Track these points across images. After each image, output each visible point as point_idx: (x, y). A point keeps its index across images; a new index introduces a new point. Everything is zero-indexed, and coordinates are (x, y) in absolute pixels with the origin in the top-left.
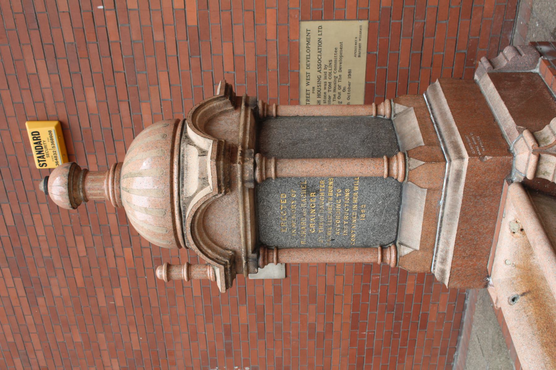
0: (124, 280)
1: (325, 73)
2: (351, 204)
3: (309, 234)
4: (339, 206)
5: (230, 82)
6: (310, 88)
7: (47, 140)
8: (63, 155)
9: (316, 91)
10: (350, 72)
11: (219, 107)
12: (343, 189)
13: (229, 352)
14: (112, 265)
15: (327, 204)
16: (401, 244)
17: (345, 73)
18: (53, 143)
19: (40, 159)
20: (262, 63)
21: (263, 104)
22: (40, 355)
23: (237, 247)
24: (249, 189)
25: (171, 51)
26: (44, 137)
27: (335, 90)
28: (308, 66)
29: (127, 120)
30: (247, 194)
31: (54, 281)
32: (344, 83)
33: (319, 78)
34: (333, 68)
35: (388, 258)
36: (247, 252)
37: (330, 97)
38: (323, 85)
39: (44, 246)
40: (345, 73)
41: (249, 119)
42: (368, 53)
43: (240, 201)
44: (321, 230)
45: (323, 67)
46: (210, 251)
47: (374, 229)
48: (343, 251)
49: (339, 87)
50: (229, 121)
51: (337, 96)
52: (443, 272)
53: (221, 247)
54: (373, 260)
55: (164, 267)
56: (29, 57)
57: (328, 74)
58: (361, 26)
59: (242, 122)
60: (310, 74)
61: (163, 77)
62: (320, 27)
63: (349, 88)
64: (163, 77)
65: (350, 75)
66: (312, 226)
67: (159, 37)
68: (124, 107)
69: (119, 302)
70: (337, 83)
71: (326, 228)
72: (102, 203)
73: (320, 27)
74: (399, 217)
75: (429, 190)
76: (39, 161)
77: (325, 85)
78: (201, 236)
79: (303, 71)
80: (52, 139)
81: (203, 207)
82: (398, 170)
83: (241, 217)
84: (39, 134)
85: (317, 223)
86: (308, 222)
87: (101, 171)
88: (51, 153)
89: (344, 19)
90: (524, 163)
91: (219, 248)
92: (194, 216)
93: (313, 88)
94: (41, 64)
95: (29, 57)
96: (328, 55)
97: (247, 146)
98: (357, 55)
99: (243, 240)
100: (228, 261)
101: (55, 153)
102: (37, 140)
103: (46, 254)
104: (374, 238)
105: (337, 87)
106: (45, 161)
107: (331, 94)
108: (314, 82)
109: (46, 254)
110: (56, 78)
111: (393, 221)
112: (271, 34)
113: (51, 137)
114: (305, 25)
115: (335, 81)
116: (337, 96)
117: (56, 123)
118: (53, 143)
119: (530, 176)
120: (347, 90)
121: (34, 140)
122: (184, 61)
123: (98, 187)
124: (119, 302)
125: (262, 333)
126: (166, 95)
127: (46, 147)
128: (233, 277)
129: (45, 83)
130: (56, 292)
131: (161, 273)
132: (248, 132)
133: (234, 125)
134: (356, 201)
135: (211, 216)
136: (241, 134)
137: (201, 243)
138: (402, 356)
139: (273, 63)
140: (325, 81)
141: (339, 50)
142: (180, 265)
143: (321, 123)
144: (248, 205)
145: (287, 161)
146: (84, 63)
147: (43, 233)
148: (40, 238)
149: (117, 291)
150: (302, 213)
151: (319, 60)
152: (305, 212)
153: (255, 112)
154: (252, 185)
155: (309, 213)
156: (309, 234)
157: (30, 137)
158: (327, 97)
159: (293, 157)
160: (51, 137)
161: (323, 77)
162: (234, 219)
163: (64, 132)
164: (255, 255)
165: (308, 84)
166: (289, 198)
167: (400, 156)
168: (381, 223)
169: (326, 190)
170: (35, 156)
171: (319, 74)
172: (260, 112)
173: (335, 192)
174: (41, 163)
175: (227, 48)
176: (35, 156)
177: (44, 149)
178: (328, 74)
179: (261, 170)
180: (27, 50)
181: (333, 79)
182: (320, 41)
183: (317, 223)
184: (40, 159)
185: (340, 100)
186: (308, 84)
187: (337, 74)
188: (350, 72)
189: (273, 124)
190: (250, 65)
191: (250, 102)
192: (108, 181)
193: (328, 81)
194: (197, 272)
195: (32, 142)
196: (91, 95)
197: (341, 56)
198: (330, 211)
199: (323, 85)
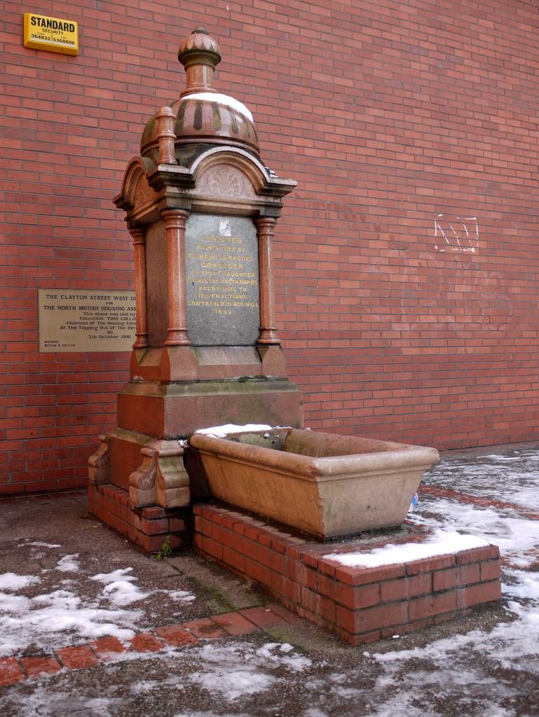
1: (127, 314)
2: (232, 301)
6: (112, 300)
7: (63, 36)
9: (108, 305)
12: (246, 293)
15: (231, 279)
19: (41, 21)
24: (258, 211)
26: (68, 35)
27: (109, 323)
29: (77, 121)
32: (116, 332)
33: (121, 309)
37: (102, 319)
38: (116, 312)
47: (206, 323)
49: (113, 328)
51: (103, 326)
56: (142, 52)
70: (116, 326)
76: (39, 19)
78: (218, 160)
80: (64, 41)
84: (71, 31)
88: (47, 34)
93: (112, 303)
95: (142, 52)
102: (65, 27)
104: (196, 324)
105: (113, 326)
106: (39, 25)
107: (106, 320)
108: (117, 303)
110: (122, 68)
111: (215, 340)
113: (67, 42)
116: (103, 326)
120: (110, 335)
121: (65, 24)
126: (104, 164)
127: (55, 32)
129: (117, 57)
134: (235, 304)
140: (119, 314)
144: (244, 207)
157: (69, 22)
160: (67, 42)
163: (69, 55)
165: (116, 298)
168: (212, 329)
169: (246, 279)
170: (46, 18)
174: (37, 20)
176: (46, 18)
177: (52, 29)
180: (150, 54)
181: (122, 322)
184: (41, 21)
185: (98, 328)
186: (116, 298)
187: (125, 325)
193: (119, 317)
195: (63, 21)
199: (116, 312)
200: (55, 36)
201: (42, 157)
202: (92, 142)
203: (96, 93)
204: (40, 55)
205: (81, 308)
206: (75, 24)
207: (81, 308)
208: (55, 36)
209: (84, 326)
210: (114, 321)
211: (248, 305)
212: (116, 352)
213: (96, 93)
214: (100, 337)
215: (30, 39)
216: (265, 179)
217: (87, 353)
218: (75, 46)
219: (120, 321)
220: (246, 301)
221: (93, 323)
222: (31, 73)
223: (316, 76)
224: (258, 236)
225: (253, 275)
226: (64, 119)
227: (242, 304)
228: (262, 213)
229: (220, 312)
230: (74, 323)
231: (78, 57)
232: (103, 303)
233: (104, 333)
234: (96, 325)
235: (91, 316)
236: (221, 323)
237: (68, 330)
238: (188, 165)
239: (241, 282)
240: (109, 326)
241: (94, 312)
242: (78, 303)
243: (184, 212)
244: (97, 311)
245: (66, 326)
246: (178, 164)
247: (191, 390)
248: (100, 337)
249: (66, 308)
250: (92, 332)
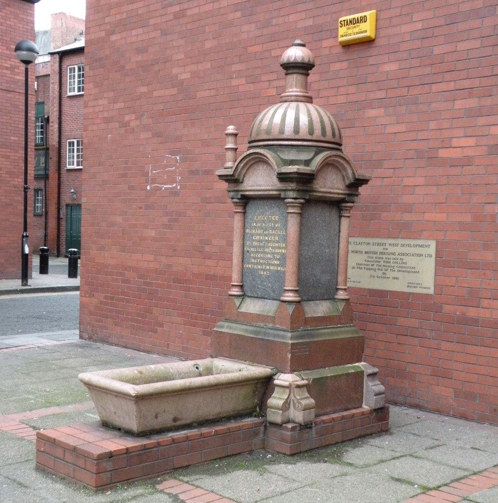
0: (251, 87)
2: (270, 265)
3: (252, 235)
5: (369, 183)
6: (387, 246)
8: (349, 41)
9: (384, 251)
10: (397, 278)
11: (347, 174)
13: (192, 172)
14: (265, 78)
16: (243, 299)
17: (396, 274)
18: (357, 33)
20: (408, 208)
21: (351, 207)
22: (196, 11)
23: (245, 184)
24: (280, 194)
25: (421, 135)
27: (384, 266)
28: (403, 245)
29: (372, 96)
31: (253, 26)
32: (390, 274)
33: (394, 254)
34: (401, 265)
35: (234, 290)
36: (241, 191)
37: (380, 262)
38: (389, 256)
39: (281, 20)
40: (396, 274)
41: (336, 196)
42: (410, 294)
43: (273, 188)
44: (255, 244)
45: (402, 257)
46: (242, 165)
48: (240, 260)
50: (335, 182)
52: (222, 327)
53: (246, 172)
54: (233, 279)
55: (235, 132)
57: (397, 261)
58: (430, 288)
59: (332, 191)
60: (397, 247)
61: (402, 128)
62: (431, 256)
63: (385, 278)
64: (402, 128)
65: (394, 278)
66: (258, 237)
67: (433, 125)
68: (381, 94)
69: (235, 82)
70: (389, 268)
71: (255, 247)
72: (283, 89)
73: (431, 256)
74: (260, 298)
75: (274, 317)
76: (344, 21)
77: (389, 259)
79: (400, 241)
81: (270, 162)
82: (288, 296)
83: (263, 188)
86: (260, 235)
87: (306, 86)
88: (350, 31)
89: (436, 275)
90: (284, 379)
91: (245, 171)
92: (264, 155)
93: (387, 249)
94: (419, 26)
96: (411, 261)
97: (312, 194)
98: (410, 285)
99: (249, 188)
100: (236, 177)
101: (350, 35)
102: (361, 20)
103: (274, 21)
107: (382, 263)
108: (391, 249)
109: (274, 21)
112: (427, 216)
114: (433, 244)
115: (391, 266)
116: (380, 267)
117: (373, 36)
118: (357, 33)
119: (276, 382)
120: (384, 276)
121: (360, 17)
122: (414, 145)
123: (294, 85)
124: (235, 82)
125: (206, 201)
127: (355, 27)
128: (227, 181)
129: (405, 28)
130: (245, 28)
131: (231, 129)
132: (324, 195)
133: (331, 185)
135: (265, 166)
136: (322, 190)
137: (247, 159)
138: (183, 315)
139: (407, 217)
141: (414, 270)
142: (236, 143)
143: (334, 247)
144: (271, 193)
145: (298, 221)
146: (416, 62)
147: (290, 20)
148: (287, 17)
149: (243, 81)
150: (265, 230)
151: (413, 255)
152: (266, 232)
153: (343, 201)
154: (282, 196)
155: (266, 235)
156: (252, 235)
157: (362, 14)
158: (380, 260)
159: (301, 225)
160: (362, 32)
161: (394, 257)
162: (263, 183)
163: (368, 42)
164: (239, 197)
165: (390, 245)
166: (276, 222)
167: (297, 299)
169: (279, 248)
171: (397, 254)
172: (344, 205)
173: (278, 253)
174: (343, 23)
175: (420, 181)
177: (353, 26)
178: (397, 261)
179: (292, 203)
182: (421, 255)
186: (390, 245)
187: (396, 269)
188: (397, 278)
189: (334, 213)
190: (407, 199)
191: (351, 198)
192: (297, 92)
193: (392, 261)
194: (230, 155)
197: (409, 272)
198: (266, 250)
199: (389, 256)
200: (356, 30)
205: (366, 253)
207: (366, 253)
208: (356, 30)
209: (367, 267)
210: (388, 264)
211: (279, 268)
212: (388, 291)
214: (378, 277)
215: (340, 39)
217: (368, 289)
219: (392, 265)
220: (278, 265)
221: (373, 265)
222: (344, 65)
229: (262, 273)
230: (360, 265)
231: (376, 40)
232: (380, 249)
233: (380, 273)
234: (375, 267)
235: (372, 260)
236: (263, 281)
237: (357, 270)
240: (384, 268)
241: (374, 256)
242: (364, 248)
244: (376, 256)
245: (356, 266)
248: (378, 277)
249: (357, 252)
250: (372, 273)
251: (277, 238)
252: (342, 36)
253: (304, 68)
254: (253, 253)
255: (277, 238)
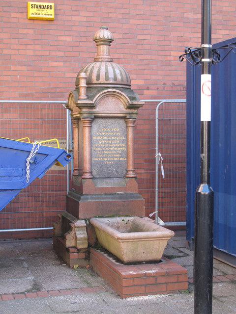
4: (113, 152)
12: (120, 154)
18: (45, 15)
29: (54, 54)
30: (124, 115)
52: (87, 199)
68: (61, 54)
76: (35, 5)
85: (104, 144)
101: (39, 14)
118: (45, 15)
129: (74, 18)
157: (49, 4)
160: (49, 15)
164: (93, 117)
173: (119, 150)
174: (34, 6)
183: (104, 144)
196: (68, 39)
200: (43, 12)
201: (36, 74)
202: (62, 64)
203: (64, 38)
204: (36, 22)
206: (52, 4)
208: (43, 12)
211: (121, 159)
213: (64, 38)
216: (128, 102)
218: (53, 17)
223: (186, 15)
224: (127, 127)
225: (124, 145)
226: (47, 53)
227: (118, 159)
228: (128, 117)
229: (108, 163)
238: (92, 100)
239: (118, 149)
243: (91, 119)
246: (88, 98)
247: (92, 198)
251: (118, 141)
252: (32, 14)
253: (109, 42)
254: (99, 151)
255: (118, 141)
